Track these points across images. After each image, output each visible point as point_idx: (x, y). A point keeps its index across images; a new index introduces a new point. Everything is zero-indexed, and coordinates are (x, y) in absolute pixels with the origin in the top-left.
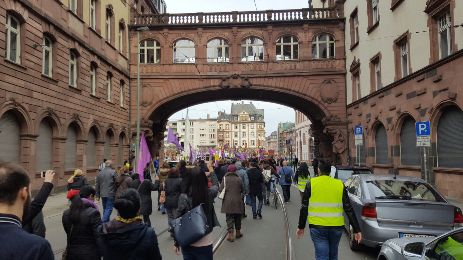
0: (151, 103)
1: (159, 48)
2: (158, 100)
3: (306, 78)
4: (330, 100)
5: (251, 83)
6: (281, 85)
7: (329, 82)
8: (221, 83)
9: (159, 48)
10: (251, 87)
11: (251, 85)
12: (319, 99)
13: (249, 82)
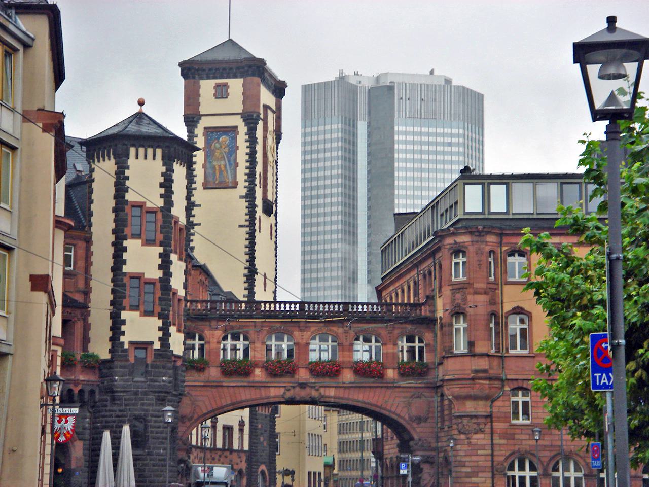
0: (192, 418)
1: (202, 342)
3: (391, 390)
4: (419, 420)
5: (323, 394)
6: (360, 398)
7: (419, 397)
8: (284, 393)
9: (202, 342)
10: (322, 400)
11: (323, 397)
12: (407, 417)
13: (320, 394)
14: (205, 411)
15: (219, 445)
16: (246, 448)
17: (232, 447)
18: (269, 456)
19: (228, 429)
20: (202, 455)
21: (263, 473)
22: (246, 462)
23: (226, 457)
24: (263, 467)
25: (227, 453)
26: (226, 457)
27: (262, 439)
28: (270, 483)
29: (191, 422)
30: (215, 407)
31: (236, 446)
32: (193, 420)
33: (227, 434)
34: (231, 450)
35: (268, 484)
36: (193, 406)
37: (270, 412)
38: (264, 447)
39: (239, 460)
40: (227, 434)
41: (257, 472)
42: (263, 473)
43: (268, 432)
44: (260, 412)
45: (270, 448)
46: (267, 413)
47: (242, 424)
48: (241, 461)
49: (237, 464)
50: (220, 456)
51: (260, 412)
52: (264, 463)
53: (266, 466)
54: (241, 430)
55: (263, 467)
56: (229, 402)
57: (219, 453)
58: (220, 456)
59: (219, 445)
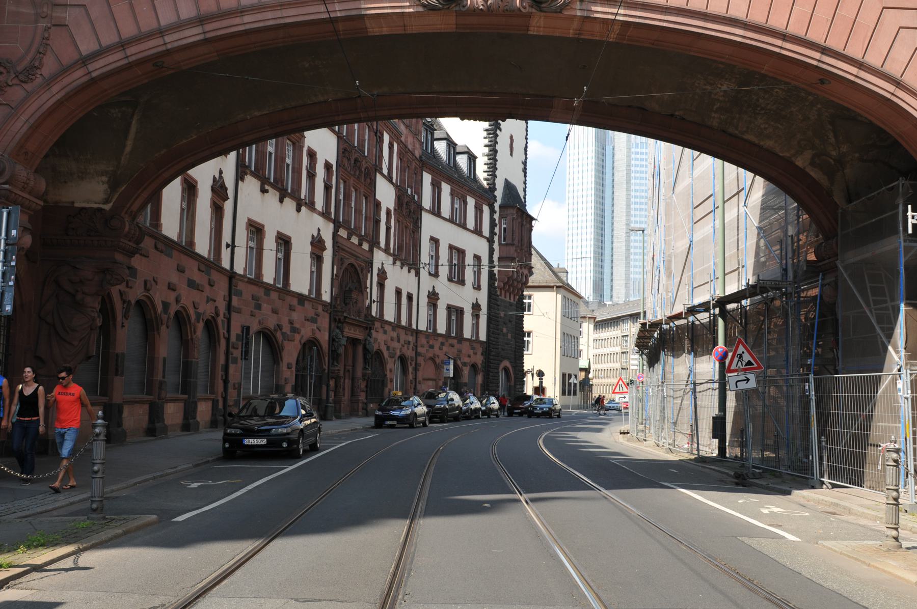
2: (69, 55)
14: (87, 46)
15: (442, 328)
16: (483, 337)
17: (462, 334)
18: (515, 351)
19: (455, 312)
20: (411, 339)
21: (506, 370)
22: (482, 354)
23: (452, 346)
24: (506, 363)
25: (455, 342)
26: (452, 346)
27: (505, 330)
28: (515, 381)
29: (29, 87)
30: (128, 30)
31: (467, 334)
32: (39, 80)
33: (453, 317)
34: (460, 337)
35: (512, 383)
36: (42, 24)
37: (516, 300)
38: (508, 339)
39: (471, 352)
40: (453, 317)
41: (498, 369)
42: (506, 370)
43: (514, 323)
44: (503, 297)
45: (516, 342)
46: (512, 301)
47: (476, 307)
48: (475, 354)
49: (469, 356)
50: (443, 344)
51: (503, 297)
52: (508, 358)
53: (511, 362)
54: (476, 316)
55: (506, 363)
56: (187, 11)
57: (440, 339)
58: (443, 344)
59: (442, 328)
